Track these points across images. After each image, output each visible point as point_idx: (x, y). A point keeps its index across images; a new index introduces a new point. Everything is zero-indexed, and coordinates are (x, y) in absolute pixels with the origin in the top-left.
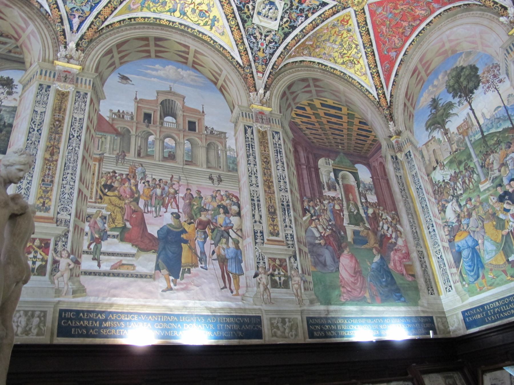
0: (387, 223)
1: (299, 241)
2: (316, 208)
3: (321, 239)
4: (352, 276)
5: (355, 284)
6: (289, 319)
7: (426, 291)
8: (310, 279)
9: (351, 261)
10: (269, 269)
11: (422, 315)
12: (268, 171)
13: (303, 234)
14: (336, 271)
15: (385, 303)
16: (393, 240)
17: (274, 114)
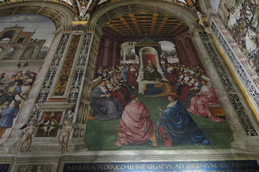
0: (188, 76)
1: (82, 97)
2: (109, 73)
3: (107, 94)
4: (137, 122)
5: (139, 128)
6: (42, 166)
7: (243, 132)
8: (84, 126)
9: (138, 109)
10: (40, 121)
11: (237, 159)
12: (72, 55)
13: (90, 91)
14: (117, 118)
15: (178, 147)
16: (196, 88)
17: (91, 25)
